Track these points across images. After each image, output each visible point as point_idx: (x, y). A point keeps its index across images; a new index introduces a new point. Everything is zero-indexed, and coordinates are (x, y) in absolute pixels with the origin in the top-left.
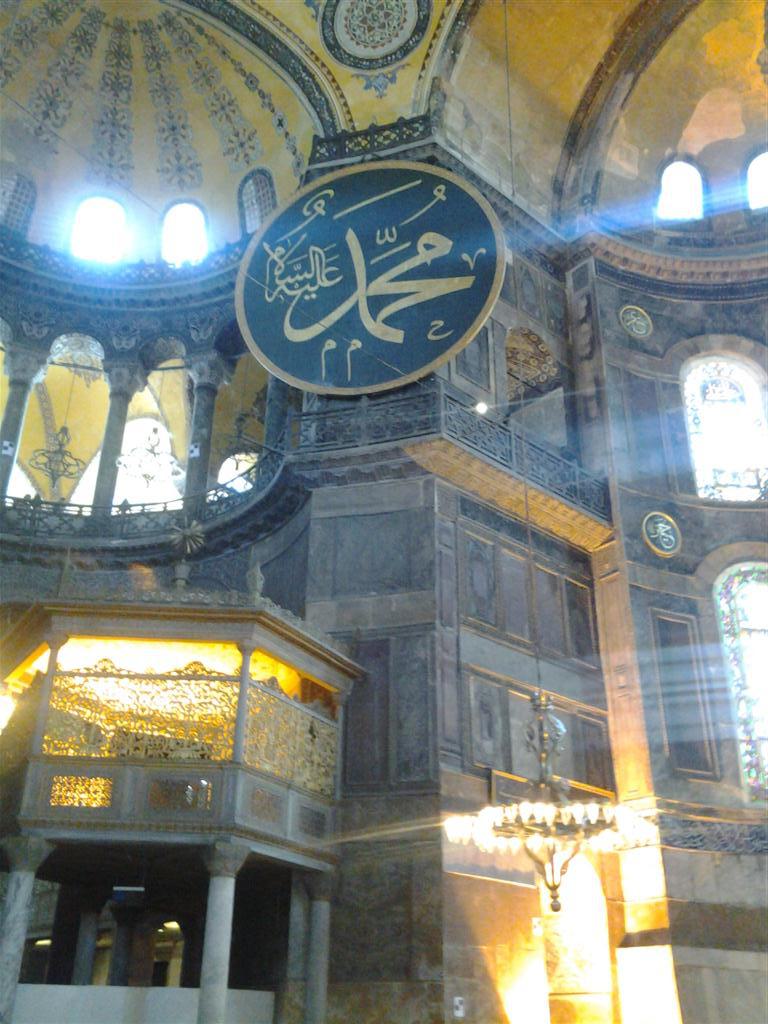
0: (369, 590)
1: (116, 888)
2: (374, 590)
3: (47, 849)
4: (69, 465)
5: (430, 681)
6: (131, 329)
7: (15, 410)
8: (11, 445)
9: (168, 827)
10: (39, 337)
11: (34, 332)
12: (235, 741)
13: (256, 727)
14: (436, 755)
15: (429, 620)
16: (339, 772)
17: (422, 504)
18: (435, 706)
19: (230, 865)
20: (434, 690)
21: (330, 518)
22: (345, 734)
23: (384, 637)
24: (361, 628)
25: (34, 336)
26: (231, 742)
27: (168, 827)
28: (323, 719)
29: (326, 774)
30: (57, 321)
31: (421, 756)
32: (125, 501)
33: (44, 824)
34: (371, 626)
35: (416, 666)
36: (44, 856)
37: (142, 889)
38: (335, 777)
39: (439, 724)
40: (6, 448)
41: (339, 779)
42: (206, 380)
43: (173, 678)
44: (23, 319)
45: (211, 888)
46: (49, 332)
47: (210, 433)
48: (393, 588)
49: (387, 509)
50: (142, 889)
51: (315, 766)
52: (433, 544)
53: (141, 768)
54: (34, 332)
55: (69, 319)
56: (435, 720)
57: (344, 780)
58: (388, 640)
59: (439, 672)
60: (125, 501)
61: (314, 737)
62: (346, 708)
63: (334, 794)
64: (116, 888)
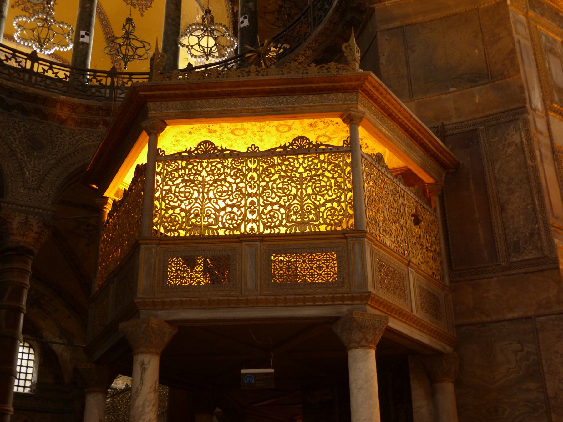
1: (243, 371)
2: (453, 86)
3: (169, 333)
4: (137, 48)
5: (529, 161)
7: (88, 5)
8: (87, 34)
12: (355, 211)
13: (371, 201)
14: (548, 231)
15: (518, 105)
16: (444, 258)
18: (539, 184)
19: (370, 337)
20: (535, 169)
21: (397, 28)
22: (444, 222)
24: (445, 122)
26: (351, 212)
28: (425, 206)
29: (434, 259)
31: (532, 234)
32: (190, 65)
33: (164, 305)
34: (454, 121)
35: (510, 151)
36: (167, 339)
37: (272, 370)
38: (441, 263)
39: (547, 200)
40: (83, 37)
43: (279, 155)
45: (351, 360)
47: (255, 5)
50: (272, 370)
51: (424, 251)
53: (258, 243)
56: (541, 199)
57: (450, 266)
58: (476, 130)
59: (537, 153)
60: (190, 65)
62: (441, 197)
63: (443, 278)
64: (243, 371)
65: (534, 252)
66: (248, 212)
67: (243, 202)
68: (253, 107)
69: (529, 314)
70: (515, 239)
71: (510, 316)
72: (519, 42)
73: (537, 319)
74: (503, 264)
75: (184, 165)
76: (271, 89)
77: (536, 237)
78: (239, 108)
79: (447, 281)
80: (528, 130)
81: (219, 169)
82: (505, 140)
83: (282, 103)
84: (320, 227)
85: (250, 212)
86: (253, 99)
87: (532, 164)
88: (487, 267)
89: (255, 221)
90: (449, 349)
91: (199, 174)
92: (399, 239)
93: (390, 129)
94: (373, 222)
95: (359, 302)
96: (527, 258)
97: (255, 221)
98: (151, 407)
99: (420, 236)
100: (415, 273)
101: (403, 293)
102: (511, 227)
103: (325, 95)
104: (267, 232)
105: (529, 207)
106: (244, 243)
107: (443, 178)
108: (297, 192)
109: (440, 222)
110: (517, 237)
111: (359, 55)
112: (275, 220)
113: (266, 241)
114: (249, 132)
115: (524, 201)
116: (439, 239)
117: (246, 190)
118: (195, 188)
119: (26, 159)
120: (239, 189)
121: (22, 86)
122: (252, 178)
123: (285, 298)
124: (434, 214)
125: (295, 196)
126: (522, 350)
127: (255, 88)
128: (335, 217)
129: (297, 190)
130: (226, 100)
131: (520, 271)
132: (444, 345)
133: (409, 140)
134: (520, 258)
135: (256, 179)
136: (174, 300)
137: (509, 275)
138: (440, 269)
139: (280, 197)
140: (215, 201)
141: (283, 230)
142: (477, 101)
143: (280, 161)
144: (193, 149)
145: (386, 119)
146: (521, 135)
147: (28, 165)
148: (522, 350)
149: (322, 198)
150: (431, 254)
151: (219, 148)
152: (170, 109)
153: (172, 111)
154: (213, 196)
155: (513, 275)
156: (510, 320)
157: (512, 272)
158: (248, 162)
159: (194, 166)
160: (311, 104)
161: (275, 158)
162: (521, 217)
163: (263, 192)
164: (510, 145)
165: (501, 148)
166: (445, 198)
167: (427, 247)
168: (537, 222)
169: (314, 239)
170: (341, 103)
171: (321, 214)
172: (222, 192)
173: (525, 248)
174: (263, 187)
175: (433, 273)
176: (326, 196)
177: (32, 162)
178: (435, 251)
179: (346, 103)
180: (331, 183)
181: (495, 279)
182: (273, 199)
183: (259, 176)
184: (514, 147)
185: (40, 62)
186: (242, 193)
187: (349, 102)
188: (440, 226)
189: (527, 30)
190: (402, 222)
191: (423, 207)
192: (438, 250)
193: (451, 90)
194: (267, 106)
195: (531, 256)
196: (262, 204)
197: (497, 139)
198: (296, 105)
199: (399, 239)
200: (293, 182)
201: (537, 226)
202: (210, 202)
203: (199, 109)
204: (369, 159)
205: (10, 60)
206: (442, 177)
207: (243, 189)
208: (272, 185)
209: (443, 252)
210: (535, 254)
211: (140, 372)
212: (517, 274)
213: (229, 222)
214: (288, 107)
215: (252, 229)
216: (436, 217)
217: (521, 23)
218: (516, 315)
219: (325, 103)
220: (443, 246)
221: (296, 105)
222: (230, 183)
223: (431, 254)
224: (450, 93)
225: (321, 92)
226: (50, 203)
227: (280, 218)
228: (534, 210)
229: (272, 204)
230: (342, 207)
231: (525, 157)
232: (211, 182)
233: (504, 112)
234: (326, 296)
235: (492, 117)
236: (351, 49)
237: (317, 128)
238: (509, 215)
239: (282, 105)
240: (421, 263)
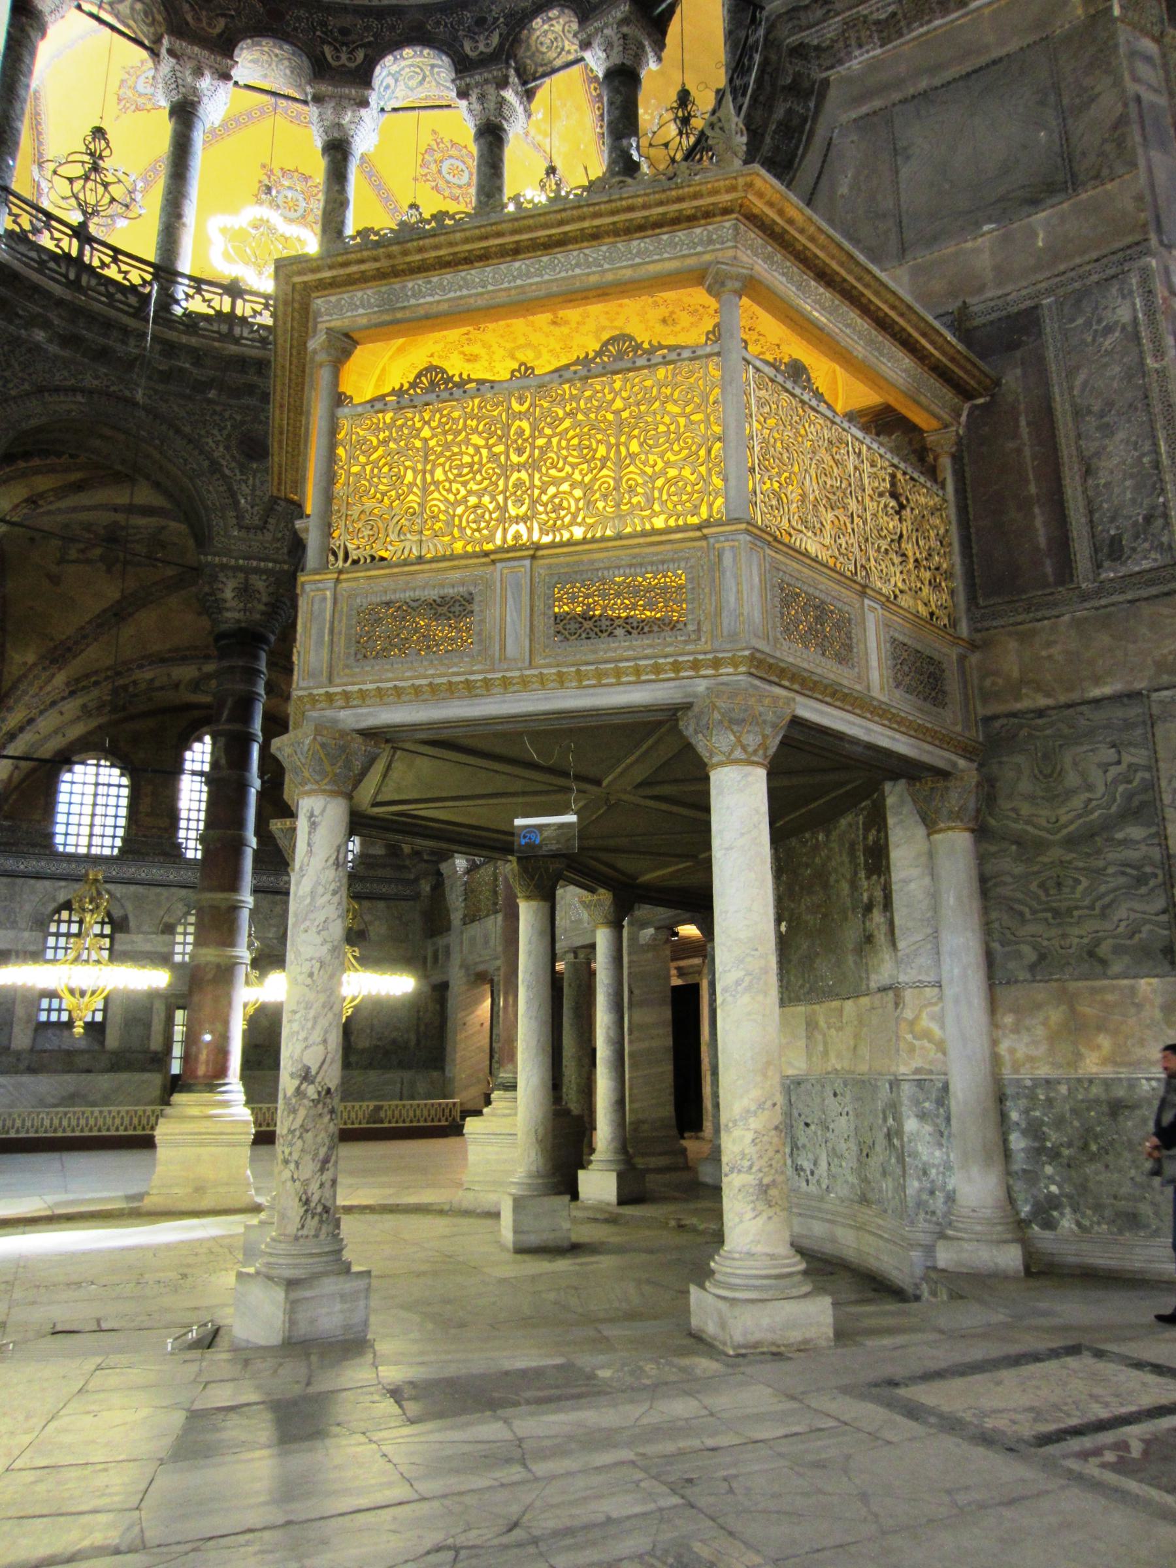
0: (978, 225)
1: (518, 822)
2: (990, 220)
6: (490, 19)
9: (600, 675)
10: (352, 65)
11: (344, 57)
15: (1130, 239)
16: (958, 583)
17: (1080, 11)
22: (962, 510)
23: (1029, 303)
25: (343, 66)
27: (600, 675)
28: (916, 475)
30: (375, 35)
31: (1148, 519)
35: (1108, 343)
37: (572, 818)
38: (952, 593)
41: (961, 598)
42: (616, 59)
44: (323, 42)
46: (366, 56)
48: (1034, 202)
49: (995, 54)
51: (911, 566)
52: (1118, 83)
54: (344, 57)
55: (392, 28)
57: (972, 599)
58: (1036, 307)
61: (902, 507)
63: (954, 624)
64: (518, 822)
65: (1153, 555)
66: (510, 502)
67: (501, 483)
68: (519, 282)
69: (1139, 685)
70: (1112, 532)
71: (1096, 692)
72: (1138, 99)
73: (1155, 696)
74: (1084, 586)
75: (388, 420)
76: (550, 236)
77: (1160, 522)
78: (490, 288)
79: (964, 629)
80: (1150, 292)
81: (456, 421)
82: (1099, 321)
83: (578, 265)
84: (654, 520)
85: (514, 502)
86: (517, 264)
87: (1156, 365)
88: (1052, 594)
89: (524, 519)
90: (962, 763)
91: (417, 436)
92: (842, 541)
93: (824, 308)
94: (774, 502)
95: (731, 670)
96: (1137, 569)
97: (524, 519)
98: (328, 897)
99: (901, 536)
100: (880, 611)
101: (845, 653)
102: (1105, 506)
103: (665, 237)
104: (546, 539)
105: (1145, 460)
106: (499, 565)
107: (963, 418)
108: (608, 453)
109: (952, 511)
110: (1118, 528)
111: (744, 139)
112: (563, 513)
113: (543, 557)
114: (544, 351)
115: (1136, 449)
116: (950, 544)
117: (508, 457)
118: (408, 463)
119: (239, 477)
120: (494, 457)
121: (216, 344)
122: (521, 431)
123: (578, 671)
124: (940, 493)
125: (604, 460)
126: (1119, 763)
127: (517, 238)
128: (684, 497)
129: (609, 447)
130: (463, 274)
131: (1121, 598)
132: (954, 757)
133: (874, 333)
134: (1123, 571)
135: (527, 433)
136: (364, 687)
137: (1097, 609)
138: (950, 603)
139: (574, 466)
140: (447, 485)
141: (578, 533)
142: (1040, 244)
143: (575, 392)
144: (406, 386)
145: (813, 283)
146: (1134, 304)
147: (244, 487)
148: (1119, 763)
149: (659, 461)
150: (928, 575)
151: (456, 379)
152: (357, 307)
153: (361, 311)
154: (442, 478)
155: (1105, 607)
156: (1097, 702)
157: (1103, 602)
158: (513, 401)
159: (407, 420)
160: (638, 260)
161: (566, 386)
162: (1128, 483)
163: (541, 458)
164: (1108, 330)
165: (1089, 339)
166: (966, 461)
167: (916, 560)
168: (1163, 491)
169: (639, 545)
170: (699, 249)
171: (656, 494)
172: (462, 466)
173: (1134, 550)
174: (541, 448)
175: (932, 614)
176: (669, 455)
177: (250, 482)
178: (937, 569)
179: (711, 247)
180: (678, 425)
181: (1067, 618)
182: (561, 470)
183: (534, 428)
184: (1117, 334)
185: (247, 297)
186: (500, 466)
187: (718, 246)
188: (953, 518)
189: (1161, 72)
190: (853, 505)
191: (912, 479)
192: (945, 566)
193: (986, 228)
194: (546, 277)
195: (1146, 565)
196: (537, 483)
197: (1080, 321)
198: (606, 266)
199: (842, 541)
200: (599, 430)
201: (1161, 500)
202: (437, 489)
203: (413, 302)
204: (770, 372)
205: (108, 266)
206: (960, 416)
207: (503, 458)
208: (559, 442)
209: (958, 569)
210: (1155, 560)
211: (307, 829)
212: (1113, 605)
213: (474, 526)
214: (588, 274)
215: (517, 537)
216: (945, 501)
217: (1148, 59)
218: (1107, 690)
219: (666, 255)
220: (957, 559)
221: (606, 266)
222: (477, 449)
223: (928, 575)
224: (983, 235)
225: (658, 231)
226: (285, 550)
227: (573, 509)
228: (1157, 465)
229: (556, 482)
230: (700, 473)
231: (1141, 352)
232: (439, 449)
233: (1097, 260)
234: (661, 661)
235: (1072, 274)
236: (721, 129)
237: (678, 328)
238: (1102, 481)
239: (578, 271)
240: (901, 591)
